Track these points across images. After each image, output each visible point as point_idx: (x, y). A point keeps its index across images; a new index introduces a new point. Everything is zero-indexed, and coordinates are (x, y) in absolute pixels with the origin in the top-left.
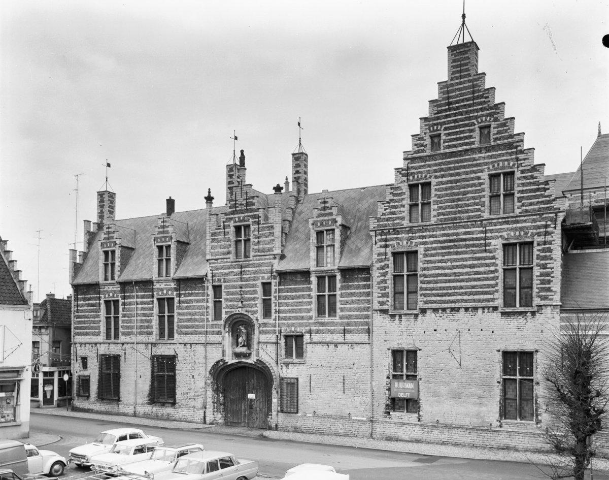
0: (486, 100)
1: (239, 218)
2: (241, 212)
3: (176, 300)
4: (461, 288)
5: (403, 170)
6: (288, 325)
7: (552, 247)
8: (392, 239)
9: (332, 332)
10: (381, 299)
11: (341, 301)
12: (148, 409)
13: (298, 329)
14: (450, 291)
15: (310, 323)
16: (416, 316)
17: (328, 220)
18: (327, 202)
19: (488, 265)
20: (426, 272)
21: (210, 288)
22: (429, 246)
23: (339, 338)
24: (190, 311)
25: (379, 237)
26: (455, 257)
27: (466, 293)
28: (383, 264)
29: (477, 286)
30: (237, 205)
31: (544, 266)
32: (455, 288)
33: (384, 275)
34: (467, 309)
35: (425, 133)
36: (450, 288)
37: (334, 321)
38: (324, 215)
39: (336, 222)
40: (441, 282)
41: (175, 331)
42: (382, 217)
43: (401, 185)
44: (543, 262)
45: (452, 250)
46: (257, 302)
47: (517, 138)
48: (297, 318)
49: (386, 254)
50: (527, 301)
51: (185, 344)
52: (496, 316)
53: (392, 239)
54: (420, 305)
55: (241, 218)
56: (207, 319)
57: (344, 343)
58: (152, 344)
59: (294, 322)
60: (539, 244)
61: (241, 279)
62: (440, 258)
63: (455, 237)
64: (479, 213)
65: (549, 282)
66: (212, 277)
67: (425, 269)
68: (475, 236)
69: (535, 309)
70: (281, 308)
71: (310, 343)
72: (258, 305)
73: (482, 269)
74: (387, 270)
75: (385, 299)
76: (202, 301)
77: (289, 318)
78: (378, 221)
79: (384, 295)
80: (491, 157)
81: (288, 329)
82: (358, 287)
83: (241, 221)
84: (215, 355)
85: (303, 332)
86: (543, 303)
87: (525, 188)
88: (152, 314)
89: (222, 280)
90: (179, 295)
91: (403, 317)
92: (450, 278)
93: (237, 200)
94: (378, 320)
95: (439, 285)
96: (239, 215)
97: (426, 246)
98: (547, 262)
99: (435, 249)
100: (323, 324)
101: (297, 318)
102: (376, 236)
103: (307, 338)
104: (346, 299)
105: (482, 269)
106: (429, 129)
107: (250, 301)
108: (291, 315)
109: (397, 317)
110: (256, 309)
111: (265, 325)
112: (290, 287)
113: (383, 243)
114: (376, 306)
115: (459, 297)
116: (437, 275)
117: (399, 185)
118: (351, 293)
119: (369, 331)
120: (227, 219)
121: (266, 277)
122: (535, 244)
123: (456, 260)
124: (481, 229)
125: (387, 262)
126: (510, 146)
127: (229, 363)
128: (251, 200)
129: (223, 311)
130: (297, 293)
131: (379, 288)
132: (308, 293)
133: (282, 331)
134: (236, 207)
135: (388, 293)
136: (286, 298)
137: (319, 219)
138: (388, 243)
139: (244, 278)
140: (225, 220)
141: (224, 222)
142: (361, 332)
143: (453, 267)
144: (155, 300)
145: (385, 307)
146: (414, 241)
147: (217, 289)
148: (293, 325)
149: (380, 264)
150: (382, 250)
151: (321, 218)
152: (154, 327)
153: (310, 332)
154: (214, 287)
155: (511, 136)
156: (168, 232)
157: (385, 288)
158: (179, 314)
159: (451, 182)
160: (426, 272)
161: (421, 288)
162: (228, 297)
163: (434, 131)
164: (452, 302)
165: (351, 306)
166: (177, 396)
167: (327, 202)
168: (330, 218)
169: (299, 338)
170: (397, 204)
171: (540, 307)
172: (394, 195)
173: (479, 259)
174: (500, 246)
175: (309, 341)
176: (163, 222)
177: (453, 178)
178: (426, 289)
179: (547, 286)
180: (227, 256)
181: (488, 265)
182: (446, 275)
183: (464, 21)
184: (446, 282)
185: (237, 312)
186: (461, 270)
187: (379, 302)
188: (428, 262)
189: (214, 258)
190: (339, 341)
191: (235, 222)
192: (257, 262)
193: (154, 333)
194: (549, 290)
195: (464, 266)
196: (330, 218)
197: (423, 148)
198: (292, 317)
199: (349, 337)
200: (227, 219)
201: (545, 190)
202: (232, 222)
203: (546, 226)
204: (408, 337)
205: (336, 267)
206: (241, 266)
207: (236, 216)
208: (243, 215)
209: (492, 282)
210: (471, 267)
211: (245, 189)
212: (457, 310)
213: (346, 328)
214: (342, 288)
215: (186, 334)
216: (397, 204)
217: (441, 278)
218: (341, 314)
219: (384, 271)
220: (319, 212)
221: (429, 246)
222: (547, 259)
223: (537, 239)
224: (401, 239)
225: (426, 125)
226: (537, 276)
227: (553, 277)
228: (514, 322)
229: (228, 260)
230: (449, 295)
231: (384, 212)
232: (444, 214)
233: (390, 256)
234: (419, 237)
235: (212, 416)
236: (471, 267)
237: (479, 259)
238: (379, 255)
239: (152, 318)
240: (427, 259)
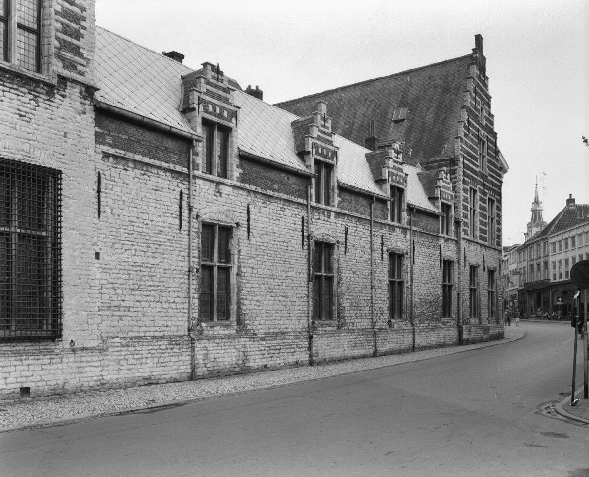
69: (54, 82)
171: (63, 80)
194: (77, 50)
226: (57, 13)
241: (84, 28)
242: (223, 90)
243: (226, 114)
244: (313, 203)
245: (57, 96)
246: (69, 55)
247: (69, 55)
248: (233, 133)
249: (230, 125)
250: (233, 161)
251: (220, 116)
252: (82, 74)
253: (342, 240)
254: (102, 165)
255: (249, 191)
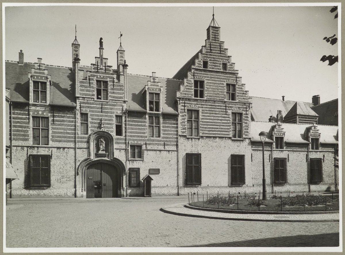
0: (225, 53)
1: (100, 76)
2: (102, 73)
3: (51, 119)
4: (217, 128)
5: (192, 73)
6: (134, 140)
7: (249, 116)
8: (188, 103)
9: (158, 145)
10: (183, 131)
11: (163, 130)
12: (26, 192)
13: (139, 142)
14: (213, 129)
15: (145, 140)
16: (199, 139)
17: (157, 88)
18: (156, 79)
19: (227, 120)
20: (203, 120)
21: (79, 114)
22: (204, 109)
23: (161, 148)
24: (63, 127)
25: (181, 101)
26: (215, 115)
27: (219, 131)
28: (183, 114)
29: (223, 128)
30: (99, 69)
31: (246, 123)
32: (215, 128)
33: (184, 119)
34: (220, 137)
35: (201, 59)
36: (213, 128)
37: (159, 139)
38: (154, 85)
39: (160, 90)
40: (209, 125)
41: (50, 139)
42: (182, 92)
43: (191, 79)
44: (246, 121)
45: (213, 112)
46: (113, 126)
47: (236, 72)
48: (138, 136)
49: (185, 110)
50: (240, 136)
51: (58, 148)
52: (230, 141)
53: (188, 103)
54: (201, 134)
55: (102, 77)
56: (77, 133)
57: (165, 151)
58: (28, 147)
59: (136, 138)
60: (244, 115)
61: (102, 112)
62: (209, 115)
63: (214, 107)
64: (223, 98)
65: (248, 129)
66: (80, 108)
67: (202, 119)
68: (222, 107)
70: (129, 130)
71: (146, 150)
72: (114, 128)
73: (225, 122)
74: (185, 117)
75: (184, 131)
76: (72, 122)
77: (134, 136)
78: (181, 94)
79: (184, 129)
80: (227, 77)
81: (133, 142)
82: (171, 124)
83: (102, 78)
84: (82, 155)
85: (142, 144)
86: (246, 137)
87: (239, 92)
88: (28, 127)
89: (88, 111)
90: (54, 116)
91: (193, 140)
92: (213, 124)
93: (99, 66)
94: (181, 140)
95: (209, 126)
96: (101, 75)
97: (203, 109)
98: (247, 121)
99: (206, 110)
100: (153, 140)
101: (138, 136)
102: (179, 101)
103: (144, 147)
104: (165, 129)
105: (225, 122)
106: (203, 58)
107: (108, 125)
108: (134, 134)
109: (190, 139)
110: (112, 130)
111: (118, 139)
112: (134, 119)
113: (183, 105)
114: (180, 133)
115: (217, 132)
116: (208, 122)
117: (190, 79)
118: (168, 126)
119: (177, 145)
120: (91, 75)
121: (119, 113)
122: (243, 114)
123: (215, 117)
124: (224, 105)
125: (185, 114)
126: (234, 74)
127: (93, 160)
128: (109, 68)
129: (89, 129)
130: (138, 124)
131: (181, 125)
132: (144, 124)
133: (130, 143)
134: (98, 70)
135: (186, 128)
136: (131, 125)
137: (151, 87)
138: (186, 105)
139: (104, 111)
140: (90, 75)
141: (89, 76)
142: (172, 145)
143: (214, 120)
144: (31, 119)
145: (184, 134)
146: (197, 106)
147: (84, 115)
148: (136, 140)
149: (182, 114)
150: (183, 108)
151: (153, 87)
152: (30, 135)
153: (146, 144)
154: (82, 114)
155: (234, 70)
156: (44, 73)
157: (185, 125)
158: (53, 128)
159: (213, 83)
160: (203, 120)
161: (201, 127)
162: (93, 121)
163: (205, 59)
164: (214, 134)
165: (168, 132)
166: (51, 182)
167: (156, 79)
168: (157, 87)
169: (140, 147)
170: (189, 88)
171: (245, 138)
172: (188, 83)
173: (224, 117)
174: (231, 113)
175: (145, 149)
176: (40, 66)
177: (213, 82)
178: (203, 128)
179: (247, 131)
180: (92, 97)
181: (227, 120)
182: (211, 122)
183: (213, 17)
184: (213, 125)
185: (101, 130)
186: (217, 121)
187: (181, 132)
188: (204, 116)
189: (82, 96)
190: (162, 149)
191: (97, 77)
192: (113, 103)
193: (30, 140)
194: (247, 132)
195: (218, 120)
196: (157, 87)
197: (201, 65)
198: (135, 136)
199: (167, 148)
200: (91, 75)
201: (246, 94)
202: (95, 77)
203: (246, 108)
204: (195, 148)
205: (160, 113)
206: (102, 104)
207: (98, 74)
208: (103, 75)
209: (229, 127)
210: (221, 120)
211: (104, 61)
212: (215, 137)
213: (165, 143)
214: (164, 123)
215: (60, 141)
216: (189, 88)
217: (209, 124)
218: (163, 136)
219: (184, 117)
220: (152, 83)
221: (204, 109)
222: (247, 120)
223: (244, 112)
224: (192, 104)
225: (202, 56)
227: (249, 127)
228: (238, 143)
229: (93, 99)
230: (213, 131)
231: (184, 90)
232: (210, 96)
233: (186, 111)
234: (199, 104)
235: (81, 193)
236: (221, 120)
237: (224, 117)
238: (181, 109)
239: (28, 129)
240: (203, 114)
241: (249, 127)
242: (281, 129)
243: (282, 134)
244: (311, 150)
245: (244, 141)
246: (246, 134)
247: (246, 134)
248: (284, 138)
249: (283, 136)
250: (284, 144)
251: (280, 135)
252: (248, 136)
253: (323, 158)
254: (253, 152)
255: (289, 151)
